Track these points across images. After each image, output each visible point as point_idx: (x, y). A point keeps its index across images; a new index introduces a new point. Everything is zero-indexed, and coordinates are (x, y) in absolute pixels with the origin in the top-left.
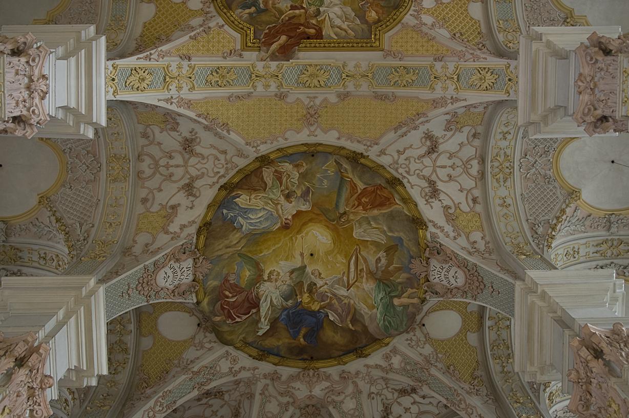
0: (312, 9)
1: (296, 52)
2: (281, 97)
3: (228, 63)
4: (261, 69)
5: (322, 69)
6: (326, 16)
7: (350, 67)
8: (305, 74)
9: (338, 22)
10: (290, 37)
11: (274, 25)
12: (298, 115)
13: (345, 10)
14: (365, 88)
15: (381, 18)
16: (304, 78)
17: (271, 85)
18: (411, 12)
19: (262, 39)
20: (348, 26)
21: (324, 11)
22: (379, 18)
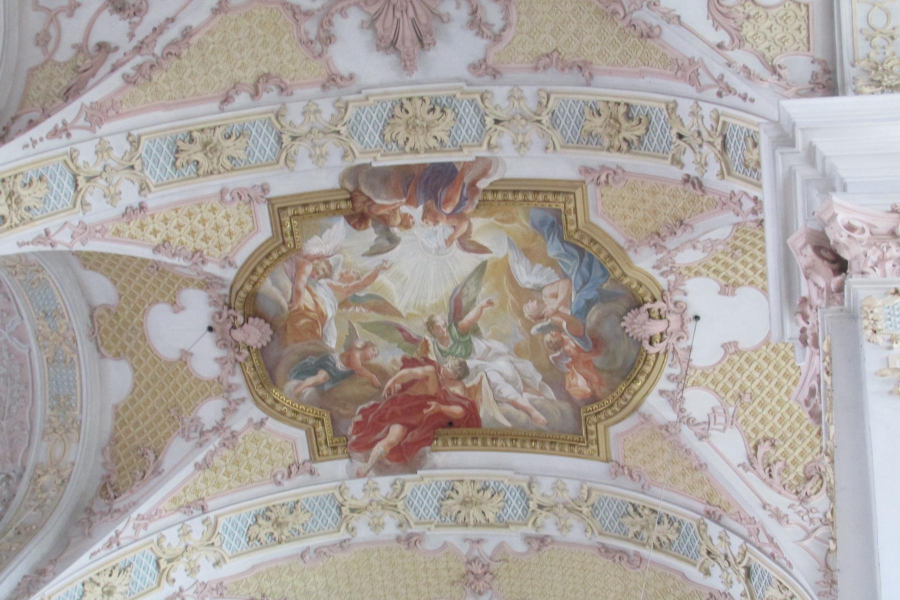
0: (450, 365)
1: (428, 455)
2: (410, 541)
3: (289, 493)
4: (360, 495)
5: (487, 488)
6: (482, 378)
7: (544, 489)
8: (452, 498)
9: (508, 391)
10: (410, 428)
11: (372, 403)
12: (451, 573)
13: (520, 366)
14: (577, 534)
15: (598, 394)
16: (453, 505)
17: (384, 524)
18: (663, 384)
19: (350, 436)
20: (531, 401)
21: (477, 367)
22: (593, 391)
